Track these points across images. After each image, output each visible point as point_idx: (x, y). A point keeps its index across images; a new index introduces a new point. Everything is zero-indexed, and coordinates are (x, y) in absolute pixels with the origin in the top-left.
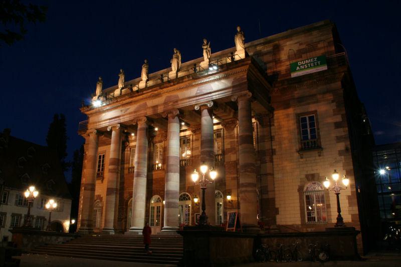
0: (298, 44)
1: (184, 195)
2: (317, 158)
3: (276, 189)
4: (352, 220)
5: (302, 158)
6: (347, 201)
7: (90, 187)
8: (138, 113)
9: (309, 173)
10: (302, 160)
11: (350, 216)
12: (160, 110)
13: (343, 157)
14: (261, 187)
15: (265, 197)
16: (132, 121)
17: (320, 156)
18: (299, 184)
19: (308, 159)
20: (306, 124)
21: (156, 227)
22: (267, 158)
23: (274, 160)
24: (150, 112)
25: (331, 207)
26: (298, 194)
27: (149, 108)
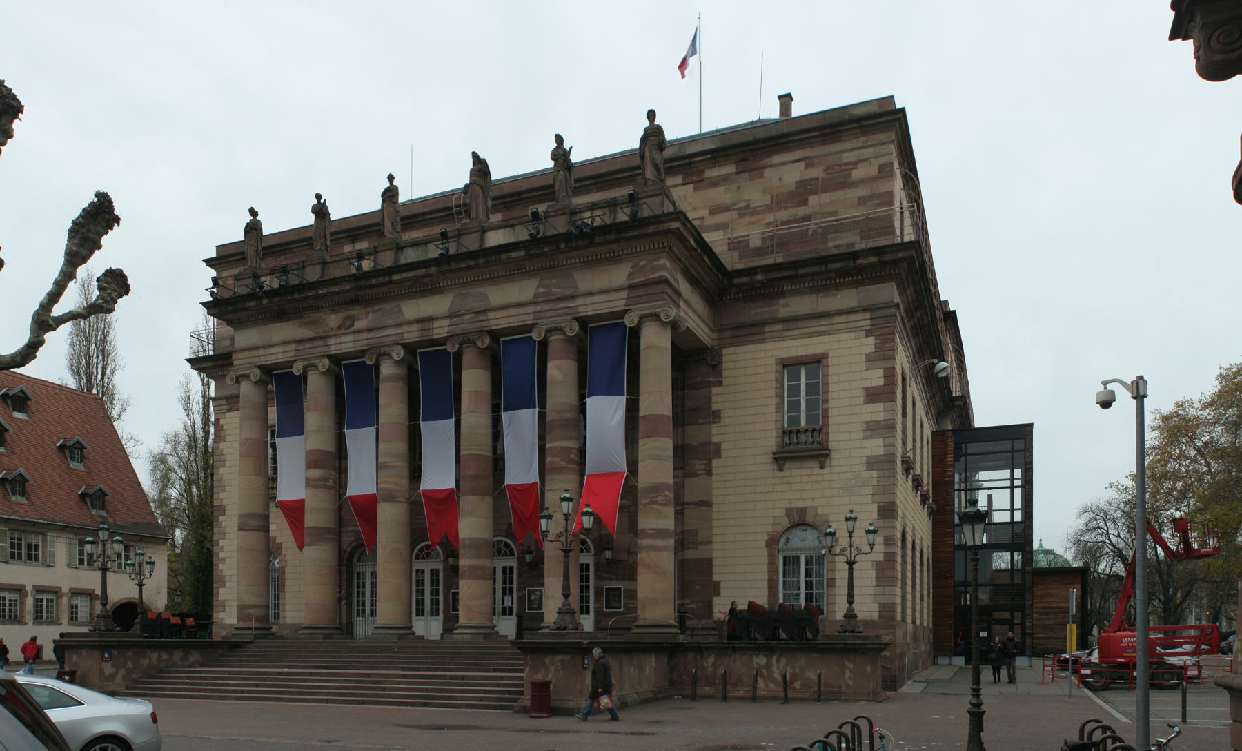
0: (802, 164)
1: (500, 542)
2: (817, 471)
3: (715, 539)
5: (781, 470)
7: (255, 523)
8: (379, 334)
9: (793, 506)
10: (781, 474)
12: (440, 330)
13: (875, 474)
14: (683, 532)
15: (690, 554)
16: (361, 353)
17: (822, 467)
18: (770, 529)
19: (794, 472)
20: (799, 385)
22: (699, 465)
23: (715, 471)
24: (412, 334)
26: (765, 552)
27: (410, 323)
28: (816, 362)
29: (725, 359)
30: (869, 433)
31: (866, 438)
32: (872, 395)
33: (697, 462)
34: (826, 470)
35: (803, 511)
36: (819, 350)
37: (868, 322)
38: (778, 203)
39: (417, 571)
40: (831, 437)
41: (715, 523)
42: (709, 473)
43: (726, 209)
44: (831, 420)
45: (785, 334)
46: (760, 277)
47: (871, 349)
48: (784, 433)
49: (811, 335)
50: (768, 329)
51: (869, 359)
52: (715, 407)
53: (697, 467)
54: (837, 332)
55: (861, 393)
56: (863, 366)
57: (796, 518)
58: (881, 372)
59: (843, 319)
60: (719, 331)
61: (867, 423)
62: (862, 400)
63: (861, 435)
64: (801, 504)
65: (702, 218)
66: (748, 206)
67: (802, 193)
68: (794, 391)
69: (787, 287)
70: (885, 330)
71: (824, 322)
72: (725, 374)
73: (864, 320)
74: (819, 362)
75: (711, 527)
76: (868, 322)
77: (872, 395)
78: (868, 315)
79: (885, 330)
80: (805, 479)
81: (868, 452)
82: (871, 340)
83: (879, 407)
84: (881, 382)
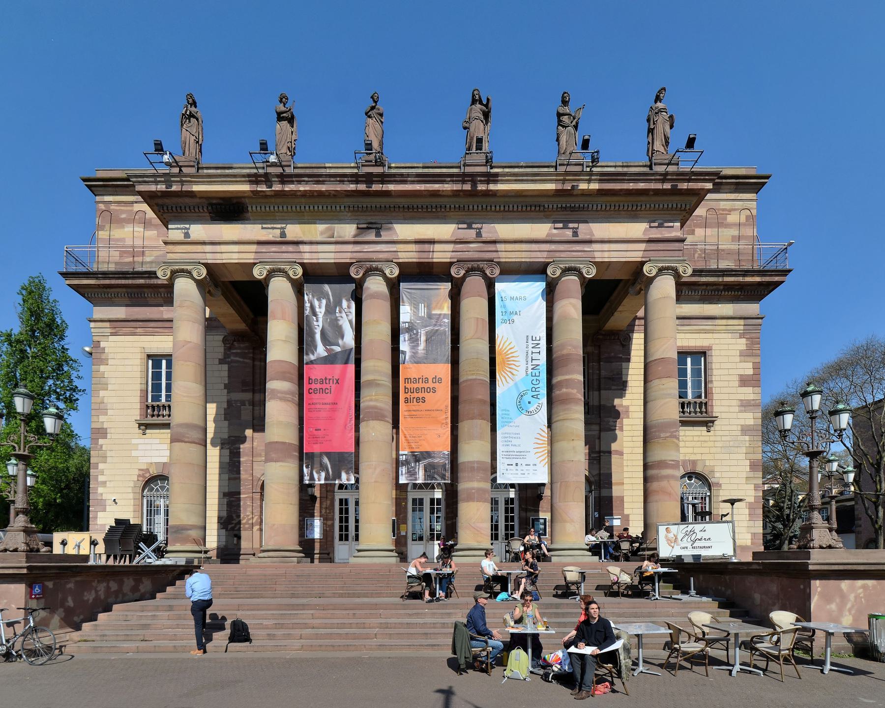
2: (705, 433)
3: (625, 481)
13: (747, 438)
19: (688, 433)
21: (354, 543)
28: (700, 354)
32: (744, 381)
34: (712, 433)
35: (694, 463)
37: (742, 328)
39: (341, 500)
40: (716, 409)
41: (625, 469)
44: (715, 397)
47: (744, 347)
51: (742, 354)
55: (737, 378)
56: (738, 359)
58: (750, 365)
59: (724, 322)
62: (737, 384)
64: (693, 457)
70: (754, 335)
71: (710, 322)
73: (739, 325)
75: (623, 472)
76: (742, 328)
77: (744, 381)
78: (742, 322)
79: (754, 335)
80: (696, 439)
81: (742, 422)
82: (744, 341)
83: (749, 390)
84: (751, 372)
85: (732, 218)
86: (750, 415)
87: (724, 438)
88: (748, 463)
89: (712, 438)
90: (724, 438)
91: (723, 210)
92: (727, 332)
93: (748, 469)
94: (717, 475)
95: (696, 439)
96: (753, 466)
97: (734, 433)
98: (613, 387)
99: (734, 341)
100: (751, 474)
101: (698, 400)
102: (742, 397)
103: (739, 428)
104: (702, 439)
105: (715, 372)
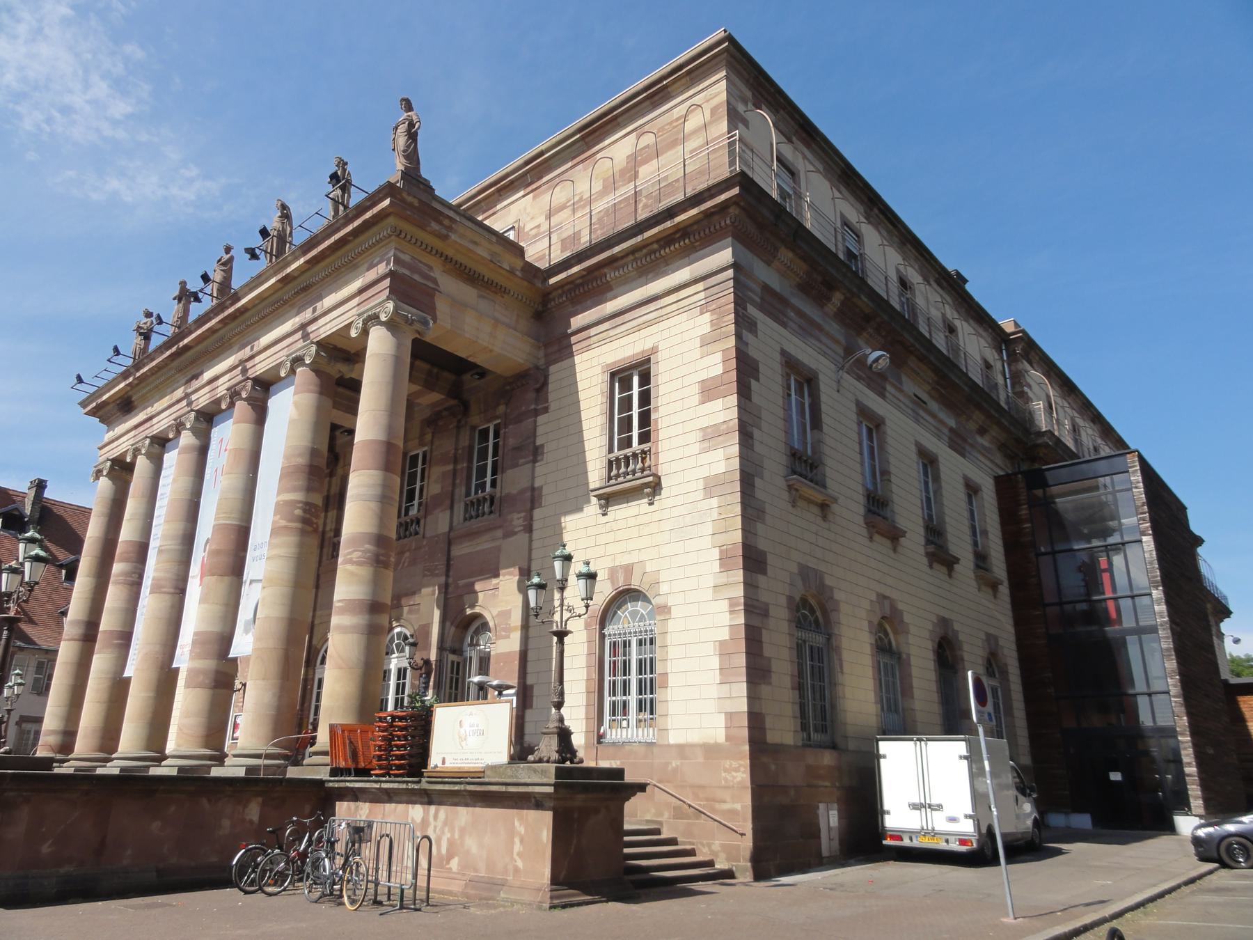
4: (728, 738)
6: (715, 662)
11: (721, 721)
13: (714, 502)
17: (651, 504)
23: (536, 525)
25: (672, 680)
29: (552, 379)
30: (706, 444)
31: (703, 452)
33: (516, 516)
36: (648, 345)
38: (611, 185)
42: (529, 529)
43: (562, 208)
45: (611, 333)
46: (575, 269)
48: (610, 463)
49: (639, 328)
50: (593, 331)
52: (538, 443)
53: (516, 522)
54: (668, 316)
55: (696, 389)
57: (621, 582)
60: (546, 346)
61: (703, 429)
62: (697, 399)
63: (696, 448)
64: (625, 560)
65: (539, 226)
66: (581, 199)
67: (636, 161)
68: (626, 404)
69: (611, 275)
71: (652, 306)
72: (551, 397)
74: (648, 360)
78: (700, 286)
82: (707, 317)
85: (690, 125)
86: (720, 454)
87: (676, 512)
88: (716, 554)
89: (656, 516)
90: (676, 512)
91: (677, 119)
92: (681, 311)
93: (716, 566)
94: (664, 589)
95: (632, 522)
96: (725, 560)
97: (692, 497)
98: (521, 461)
99: (691, 324)
100: (723, 579)
101: (628, 451)
102: (705, 422)
103: (701, 484)
104: (641, 520)
105: (662, 390)
